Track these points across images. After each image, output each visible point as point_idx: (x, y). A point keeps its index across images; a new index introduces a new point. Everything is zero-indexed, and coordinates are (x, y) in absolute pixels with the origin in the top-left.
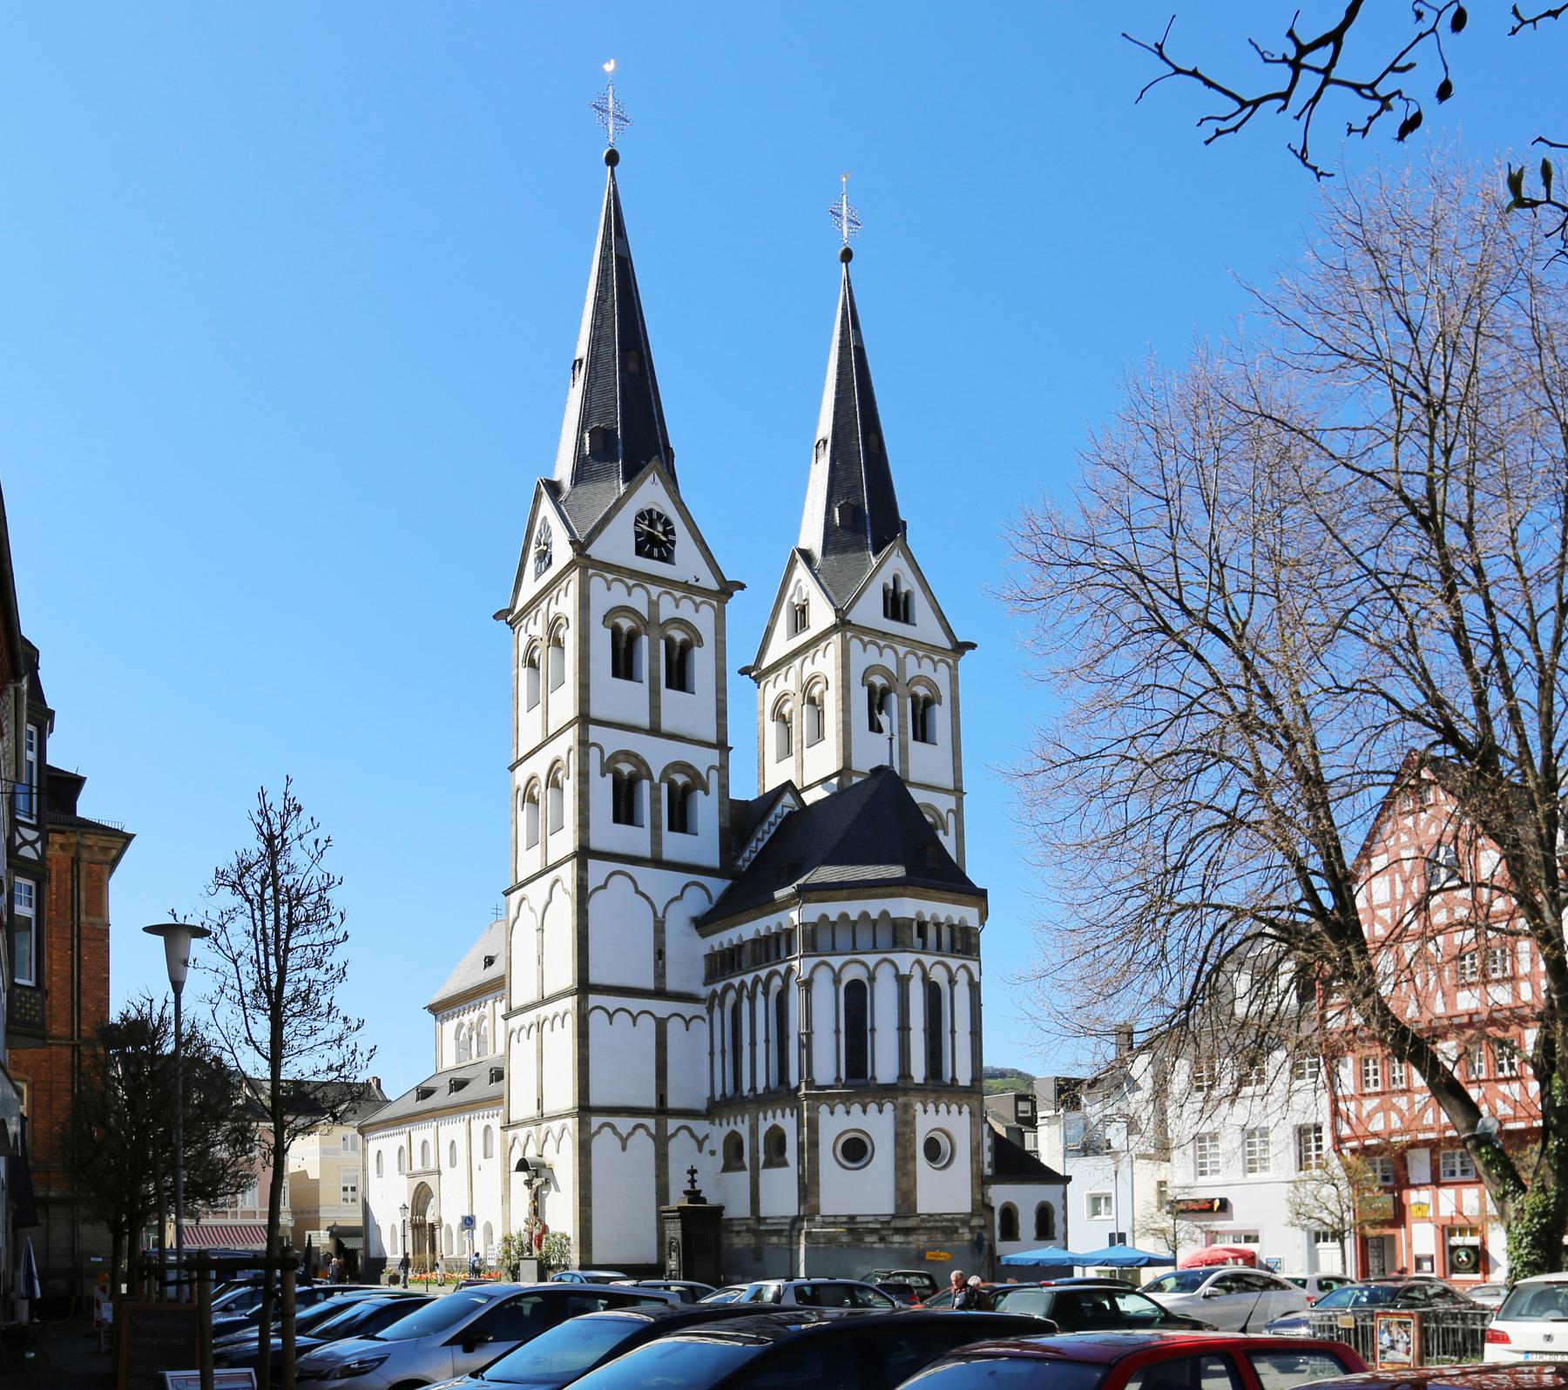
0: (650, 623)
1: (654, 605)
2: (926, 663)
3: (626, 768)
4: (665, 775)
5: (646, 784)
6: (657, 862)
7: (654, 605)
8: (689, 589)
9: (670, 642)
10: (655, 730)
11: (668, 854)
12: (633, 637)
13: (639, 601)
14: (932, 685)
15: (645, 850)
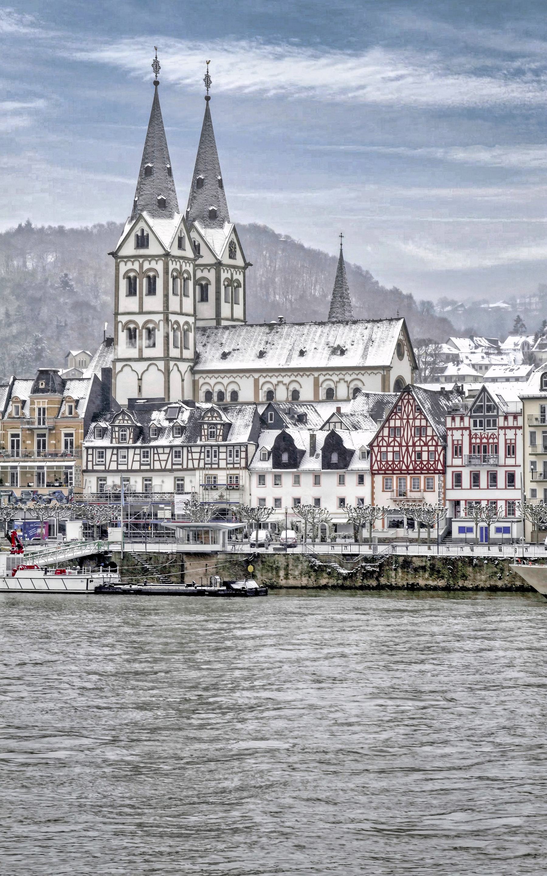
0: (143, 273)
1: (141, 266)
2: (206, 271)
3: (132, 326)
4: (143, 327)
5: (137, 331)
6: (141, 359)
7: (141, 266)
8: (153, 257)
9: (149, 277)
10: (141, 312)
11: (145, 355)
12: (135, 278)
13: (136, 266)
14: (207, 279)
15: (136, 356)
